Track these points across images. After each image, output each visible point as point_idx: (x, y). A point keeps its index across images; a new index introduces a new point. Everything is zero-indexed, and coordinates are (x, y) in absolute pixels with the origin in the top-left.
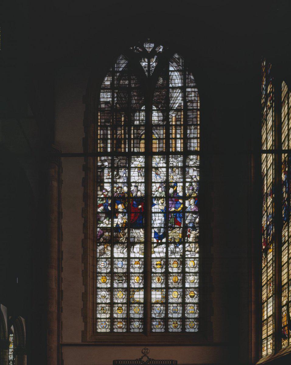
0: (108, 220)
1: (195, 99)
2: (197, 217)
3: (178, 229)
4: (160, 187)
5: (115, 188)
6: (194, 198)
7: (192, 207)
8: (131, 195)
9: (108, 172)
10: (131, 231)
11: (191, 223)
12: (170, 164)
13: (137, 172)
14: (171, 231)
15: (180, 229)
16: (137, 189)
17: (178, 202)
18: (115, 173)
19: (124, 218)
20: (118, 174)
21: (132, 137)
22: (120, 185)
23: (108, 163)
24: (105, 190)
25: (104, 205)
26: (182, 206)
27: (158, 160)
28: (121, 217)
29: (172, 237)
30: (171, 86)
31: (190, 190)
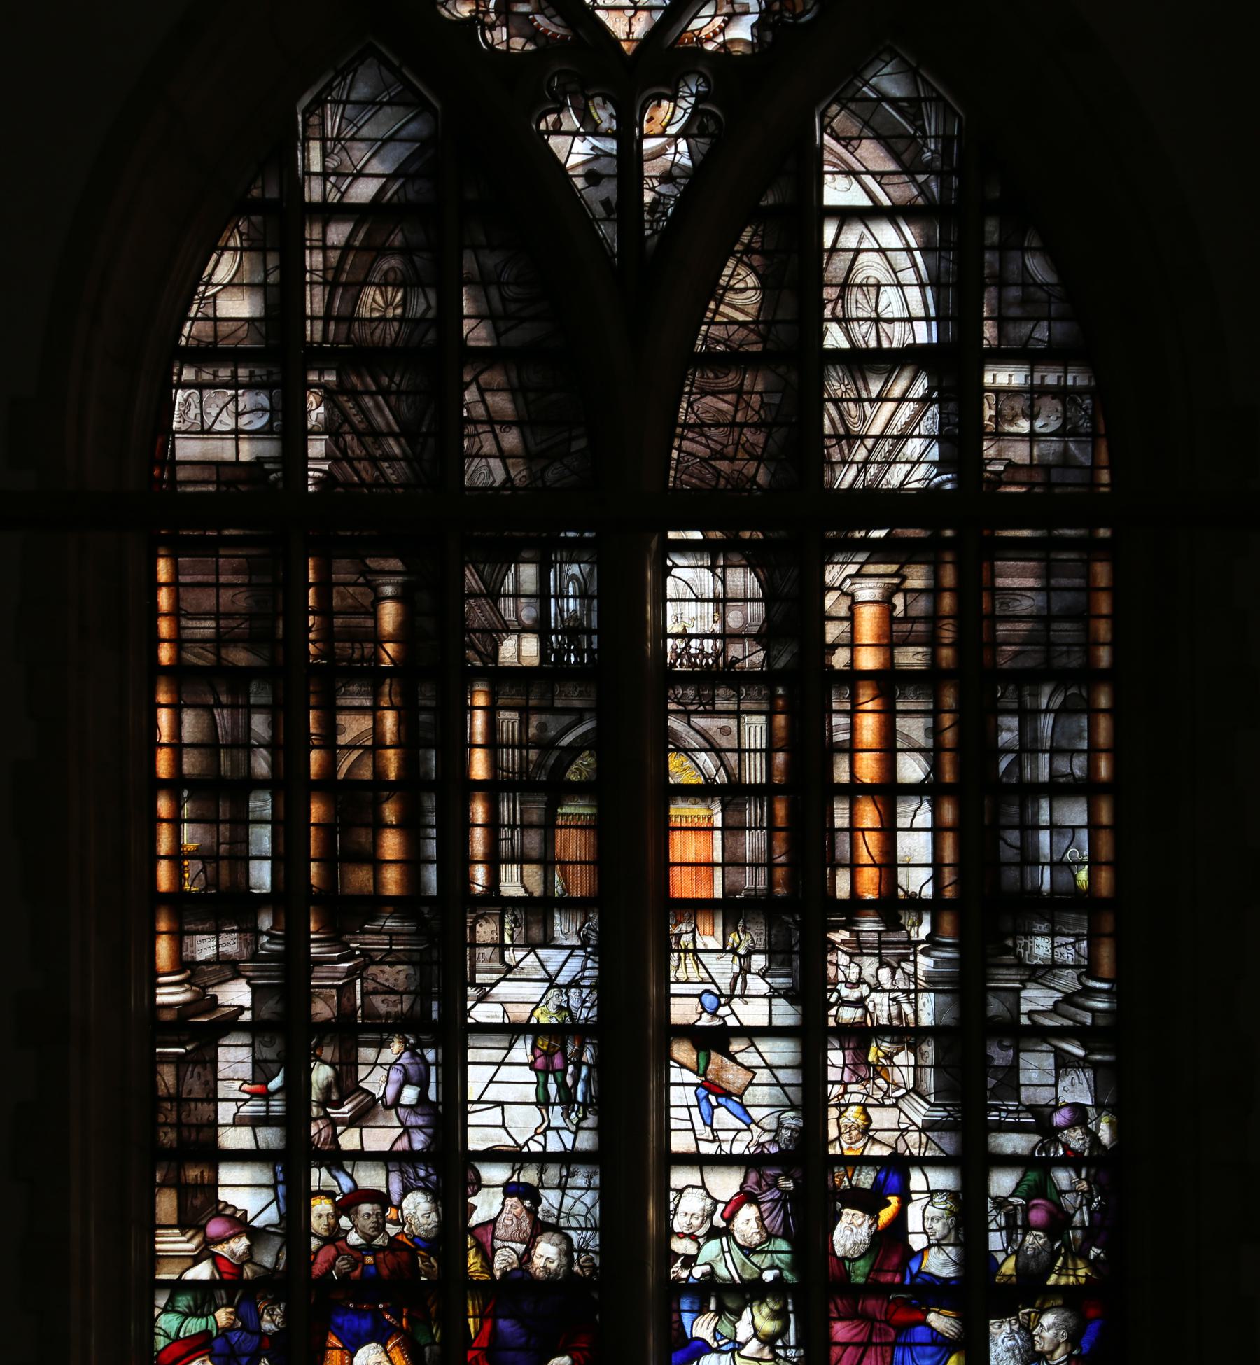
1: (1066, 450)
4: (745, 1197)
5: (321, 1207)
6: (1070, 1298)
9: (255, 1062)
12: (842, 1002)
13: (532, 1066)
16: (532, 1212)
17: (920, 1334)
18: (321, 1074)
20: (346, 1083)
21: (479, 767)
22: (371, 1177)
23: (255, 990)
25: (218, 1344)
27: (723, 969)
30: (835, 338)
31: (1027, 1228)
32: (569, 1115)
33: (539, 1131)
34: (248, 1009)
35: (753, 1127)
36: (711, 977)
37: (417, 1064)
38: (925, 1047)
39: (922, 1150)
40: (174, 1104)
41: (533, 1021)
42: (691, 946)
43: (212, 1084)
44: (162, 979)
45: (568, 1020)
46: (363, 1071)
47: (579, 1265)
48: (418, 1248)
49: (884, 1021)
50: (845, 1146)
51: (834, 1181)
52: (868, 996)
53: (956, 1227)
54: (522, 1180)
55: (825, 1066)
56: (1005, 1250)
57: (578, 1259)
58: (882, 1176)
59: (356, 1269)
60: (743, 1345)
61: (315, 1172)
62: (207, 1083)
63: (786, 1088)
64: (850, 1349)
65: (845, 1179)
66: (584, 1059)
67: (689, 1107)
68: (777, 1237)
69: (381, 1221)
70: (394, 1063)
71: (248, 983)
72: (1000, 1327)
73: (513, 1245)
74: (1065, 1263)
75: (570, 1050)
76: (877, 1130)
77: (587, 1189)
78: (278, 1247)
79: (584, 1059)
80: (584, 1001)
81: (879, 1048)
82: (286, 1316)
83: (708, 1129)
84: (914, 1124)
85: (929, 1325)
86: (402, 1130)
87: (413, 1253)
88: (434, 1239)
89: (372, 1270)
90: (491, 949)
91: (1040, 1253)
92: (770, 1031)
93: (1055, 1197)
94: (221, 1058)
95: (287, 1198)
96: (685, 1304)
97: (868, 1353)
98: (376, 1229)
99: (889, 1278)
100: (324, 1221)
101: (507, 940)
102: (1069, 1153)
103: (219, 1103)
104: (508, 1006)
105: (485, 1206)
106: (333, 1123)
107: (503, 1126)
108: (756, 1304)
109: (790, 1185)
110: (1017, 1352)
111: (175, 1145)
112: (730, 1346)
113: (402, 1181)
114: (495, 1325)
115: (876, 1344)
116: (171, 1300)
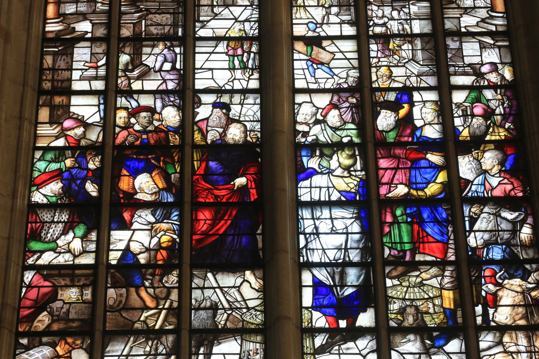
0: (84, 238)
2: (523, 222)
3: (434, 270)
4: (333, 106)
6: (499, 145)
7: (494, 182)
8: (197, 137)
9: (92, 54)
10: (197, 281)
11: (496, 243)
12: (375, 25)
13: (227, 54)
14: (398, 277)
15: (444, 271)
16: (227, 115)
17: (423, 163)
18: (124, 59)
19: (164, 226)
22: (146, 101)
23: (93, 25)
24: (76, 119)
25: (66, 175)
26: (442, 177)
28: (150, 223)
29: (408, 303)
31: (473, 116)
32: (245, 74)
33: (230, 80)
34: (90, 32)
35: (335, 77)
36: (312, 16)
37: (171, 54)
38: (416, 42)
39: (418, 84)
40: (51, 72)
41: (227, 35)
42: (302, 4)
43: (70, 64)
44: (48, 21)
45: (244, 35)
46: (144, 57)
47: (250, 137)
48: (170, 131)
49: (396, 32)
50: (380, 84)
51: (376, 98)
52: (387, 22)
53: (438, 116)
54: (222, 101)
55: (369, 51)
56: (463, 126)
57: (250, 135)
58: (399, 96)
59: (138, 140)
60: (334, 171)
61: (119, 99)
62: (67, 63)
63: (350, 61)
64: (388, 171)
65: (381, 97)
66: (252, 50)
67: (303, 69)
68: (348, 123)
69: (151, 120)
70: (160, 54)
71: (90, 22)
72: (464, 159)
73: (217, 129)
74: (493, 130)
75: (245, 47)
76: (395, 77)
77: (254, 104)
78: (99, 131)
79: (252, 50)
80: (252, 27)
81: (394, 43)
82: (102, 161)
83: (313, 78)
84: (414, 73)
85: (428, 160)
86: (163, 81)
87: (167, 133)
88: (177, 127)
89: (146, 141)
90: (207, 8)
91: (480, 126)
92: (342, 37)
93: (485, 102)
94: (75, 53)
95: (105, 110)
96: (303, 153)
97: (398, 173)
98: (148, 123)
99: (406, 139)
100: (122, 120)
101: (215, 3)
102: (490, 83)
103: (73, 71)
104: (215, 30)
105: (203, 112)
106: (129, 79)
107: (213, 78)
108: (339, 152)
109: (354, 101)
110: (473, 170)
111: (50, 88)
112: (327, 171)
113: (162, 103)
114: (207, 165)
115: (401, 168)
116: (43, 155)
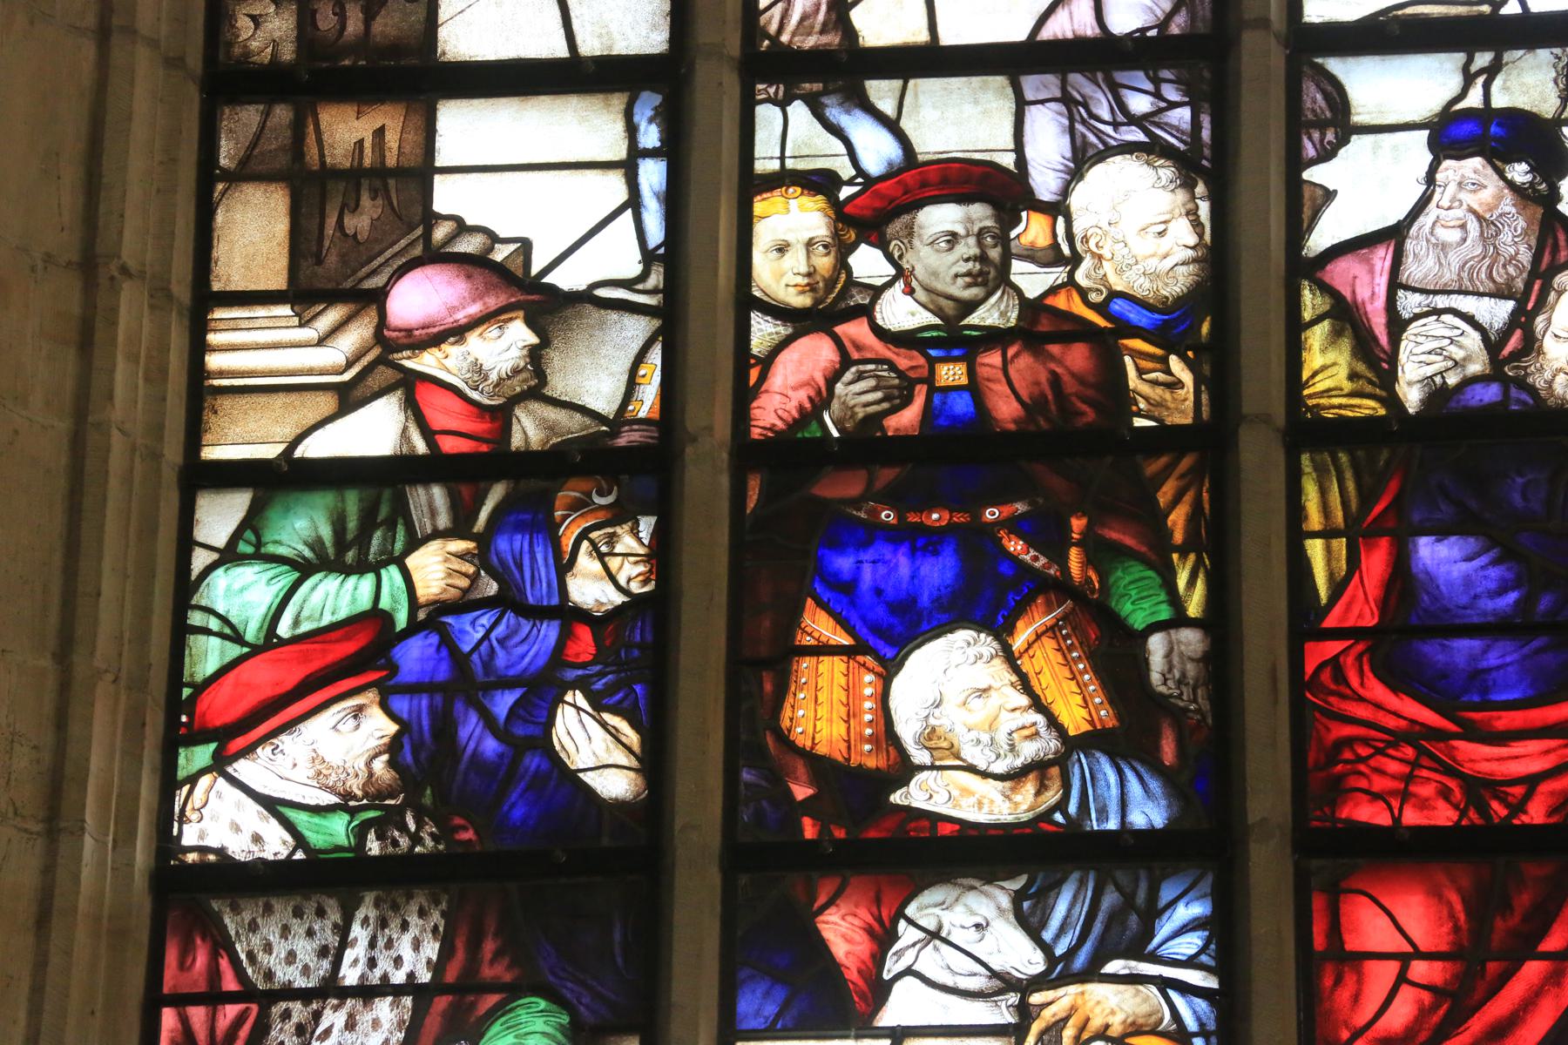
59: (907, 401)
61: (767, 117)
69: (995, 254)
82: (661, 555)
89: (962, 404)
95: (673, 200)
98: (975, 279)
100: (796, 261)
